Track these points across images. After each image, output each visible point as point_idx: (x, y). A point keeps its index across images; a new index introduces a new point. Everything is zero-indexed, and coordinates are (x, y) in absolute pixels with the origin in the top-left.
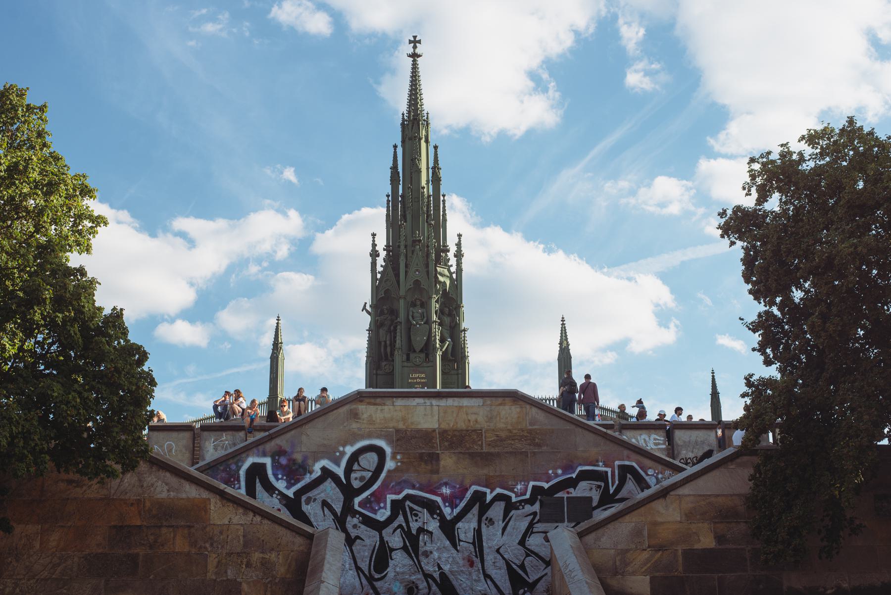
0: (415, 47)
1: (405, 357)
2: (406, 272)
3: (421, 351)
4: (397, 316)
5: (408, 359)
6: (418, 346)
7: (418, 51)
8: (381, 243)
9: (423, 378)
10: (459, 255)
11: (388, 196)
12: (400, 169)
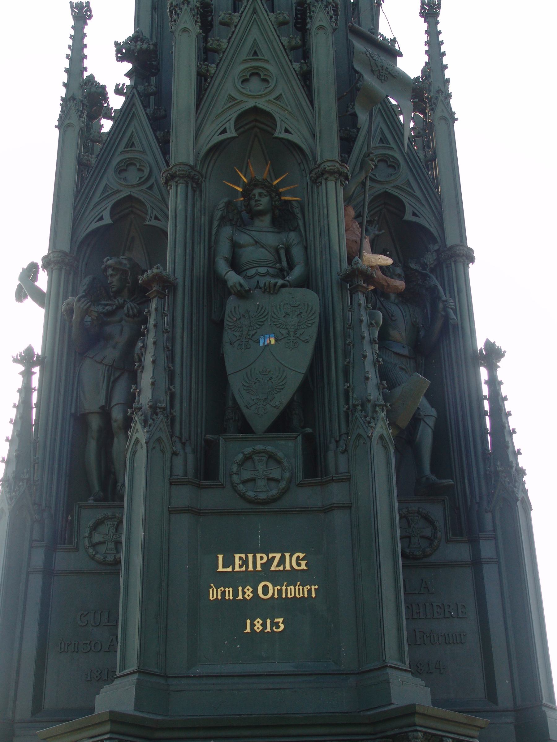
2: (203, 80)
3: (281, 425)
4: (156, 253)
5: (207, 469)
9: (292, 577)
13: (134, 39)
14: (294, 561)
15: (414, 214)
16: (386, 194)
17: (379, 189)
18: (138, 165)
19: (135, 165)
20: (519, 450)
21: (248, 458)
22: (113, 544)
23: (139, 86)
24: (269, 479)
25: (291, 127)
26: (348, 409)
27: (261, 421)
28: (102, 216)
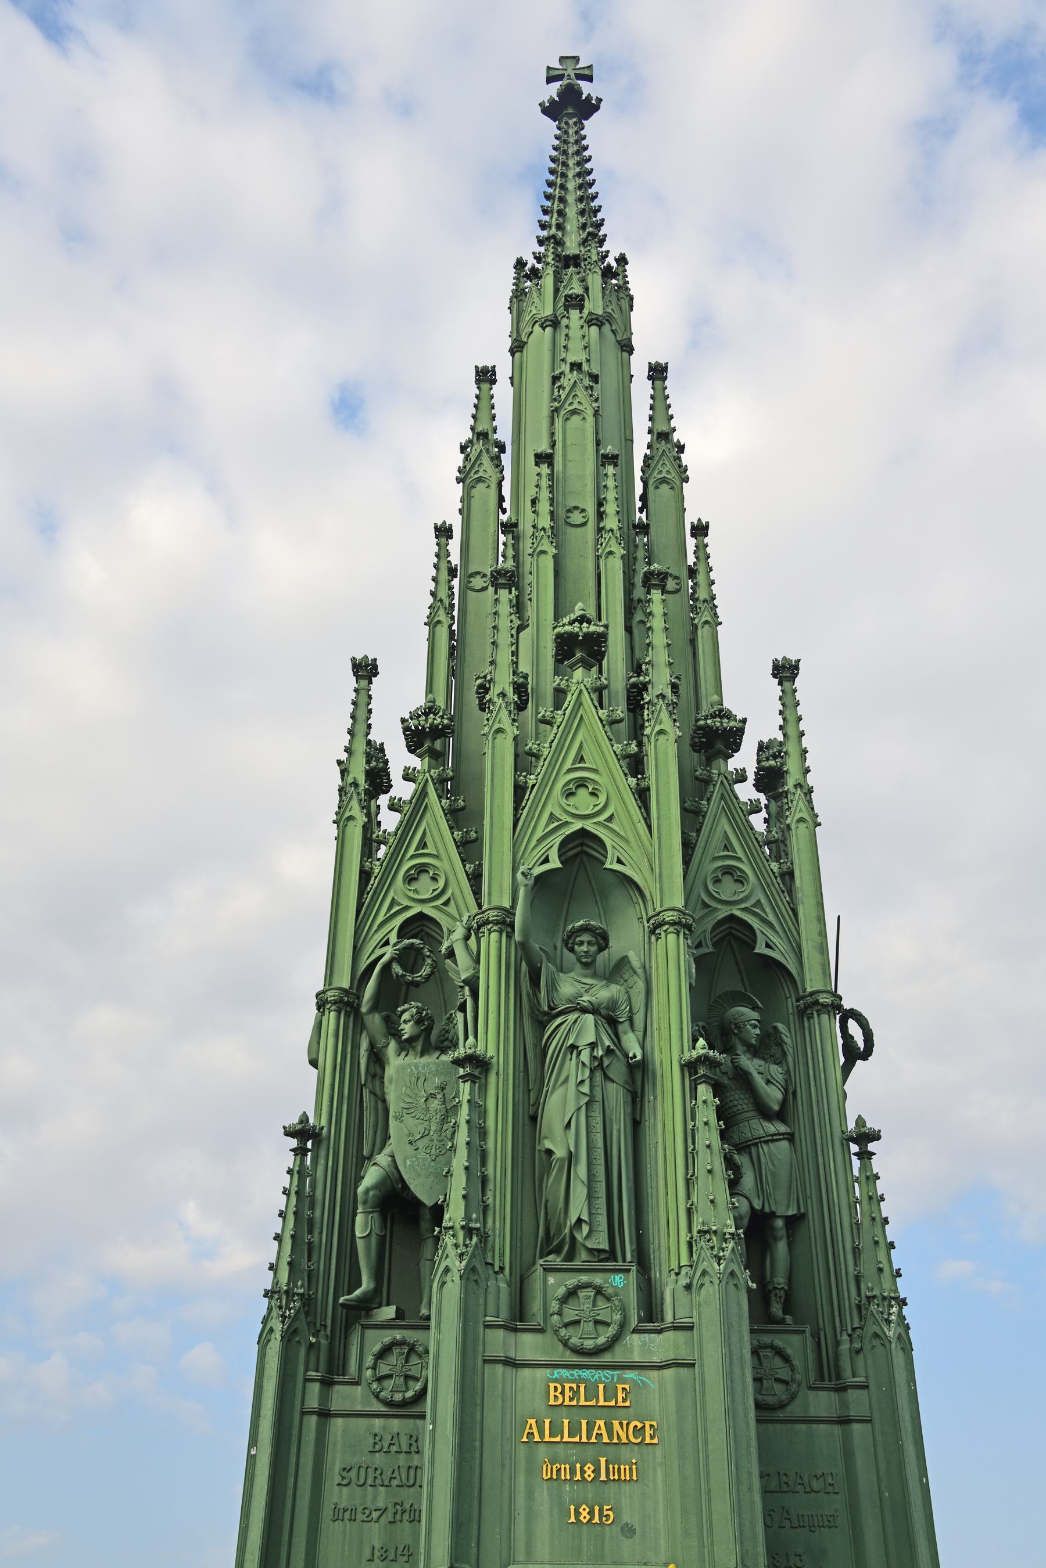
11: (443, 532)
13: (430, 710)
15: (768, 946)
16: (732, 918)
17: (723, 912)
18: (431, 873)
19: (428, 872)
20: (898, 1271)
21: (572, 1293)
22: (402, 1379)
23: (433, 771)
24: (597, 1322)
26: (691, 1238)
28: (388, 940)
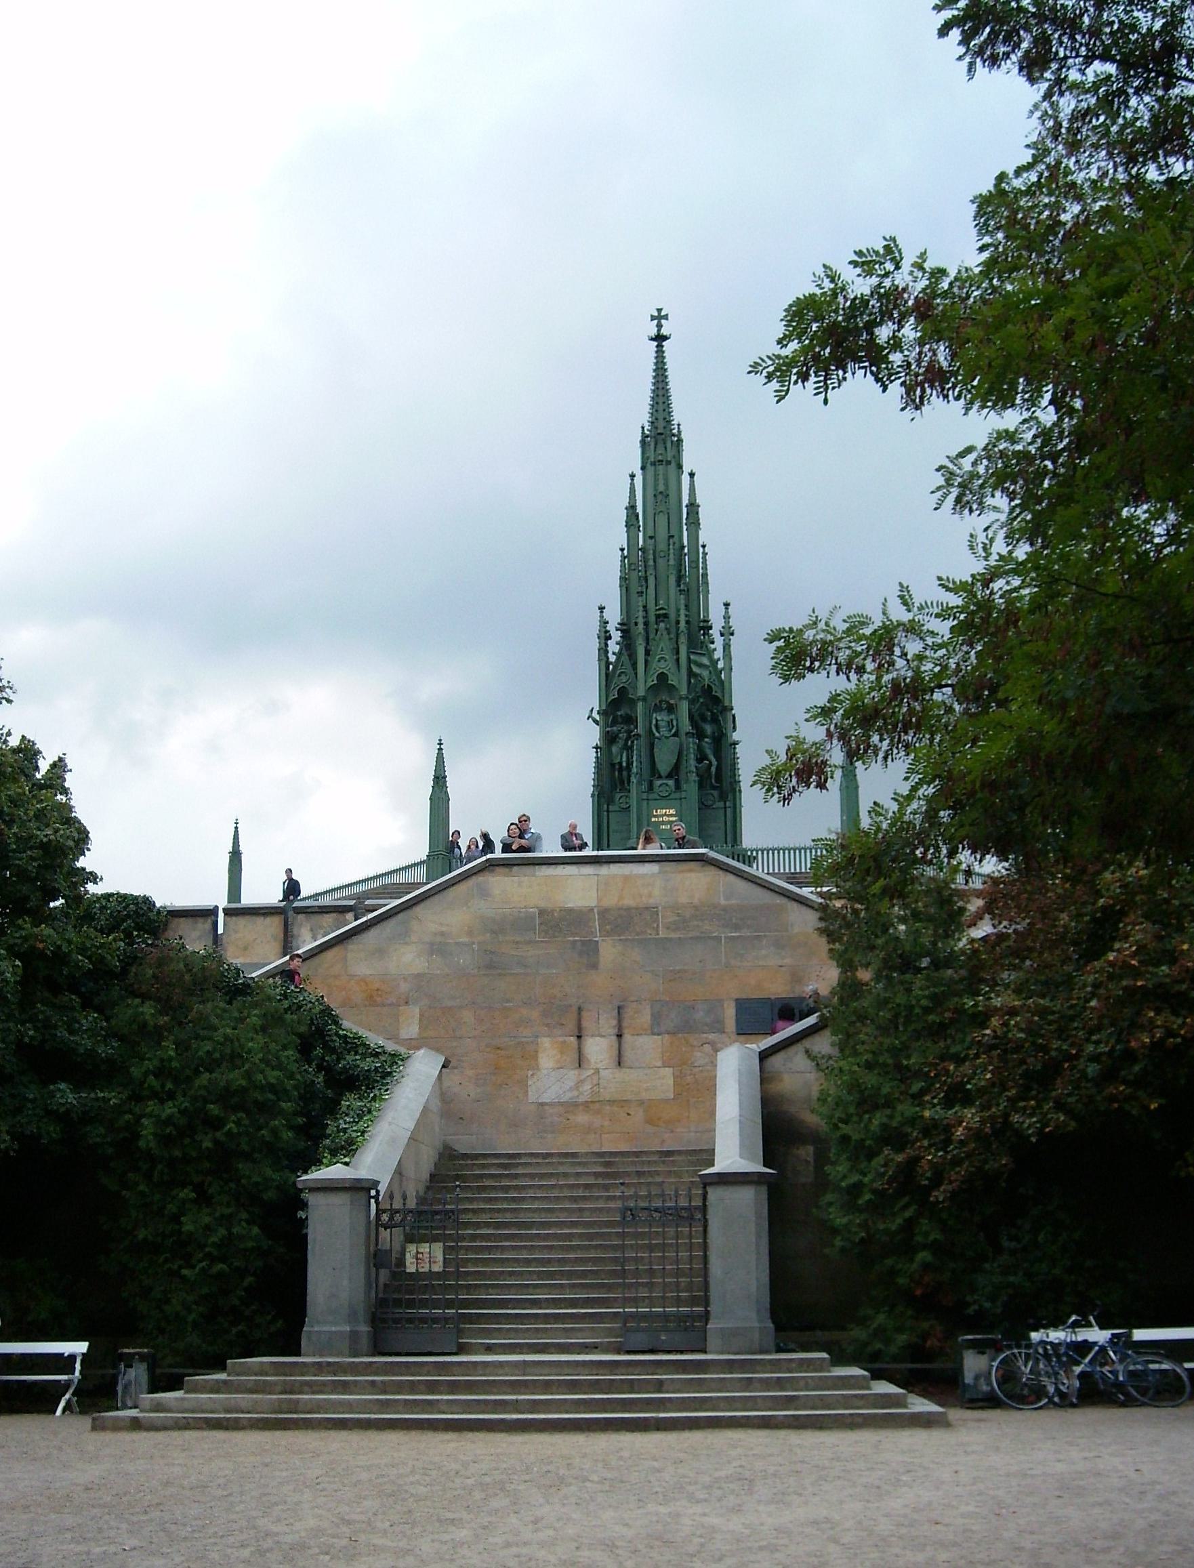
0: (659, 326)
1: (644, 787)
5: (651, 788)
6: (664, 767)
7: (664, 332)
8: (614, 616)
9: (672, 815)
10: (727, 632)
11: (622, 550)
12: (640, 510)
14: (672, 812)
25: (672, 680)
27: (663, 773)
